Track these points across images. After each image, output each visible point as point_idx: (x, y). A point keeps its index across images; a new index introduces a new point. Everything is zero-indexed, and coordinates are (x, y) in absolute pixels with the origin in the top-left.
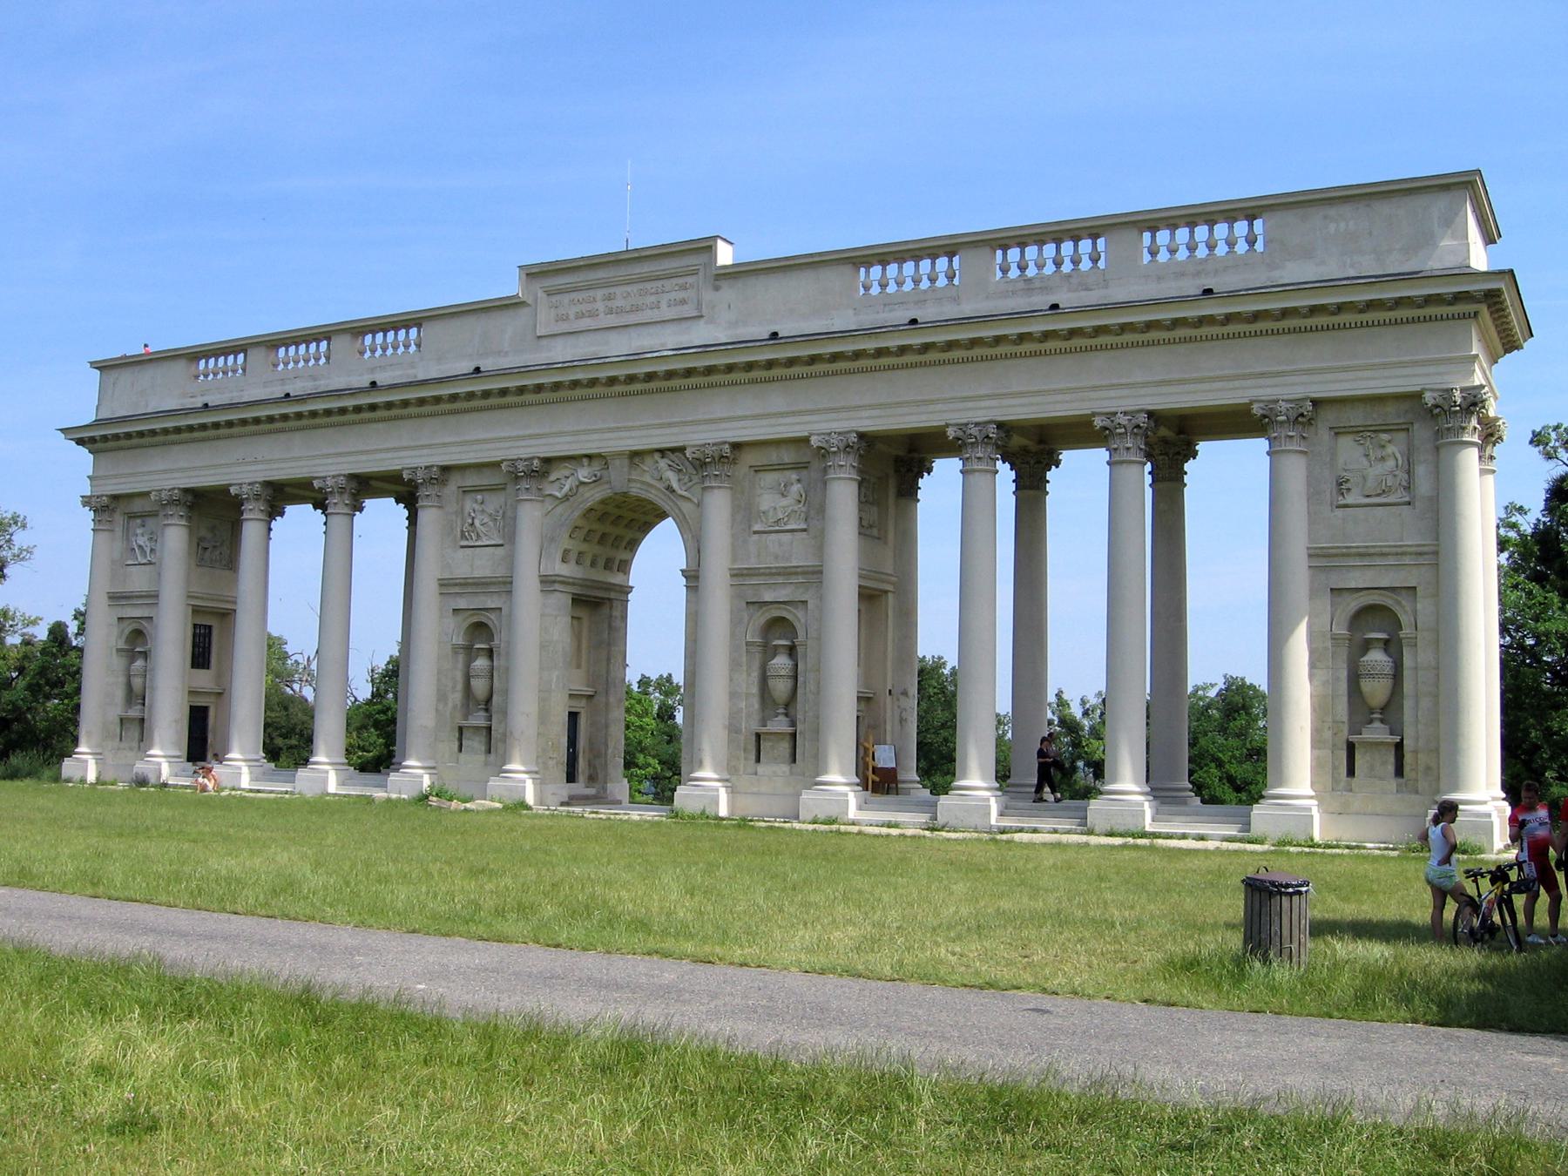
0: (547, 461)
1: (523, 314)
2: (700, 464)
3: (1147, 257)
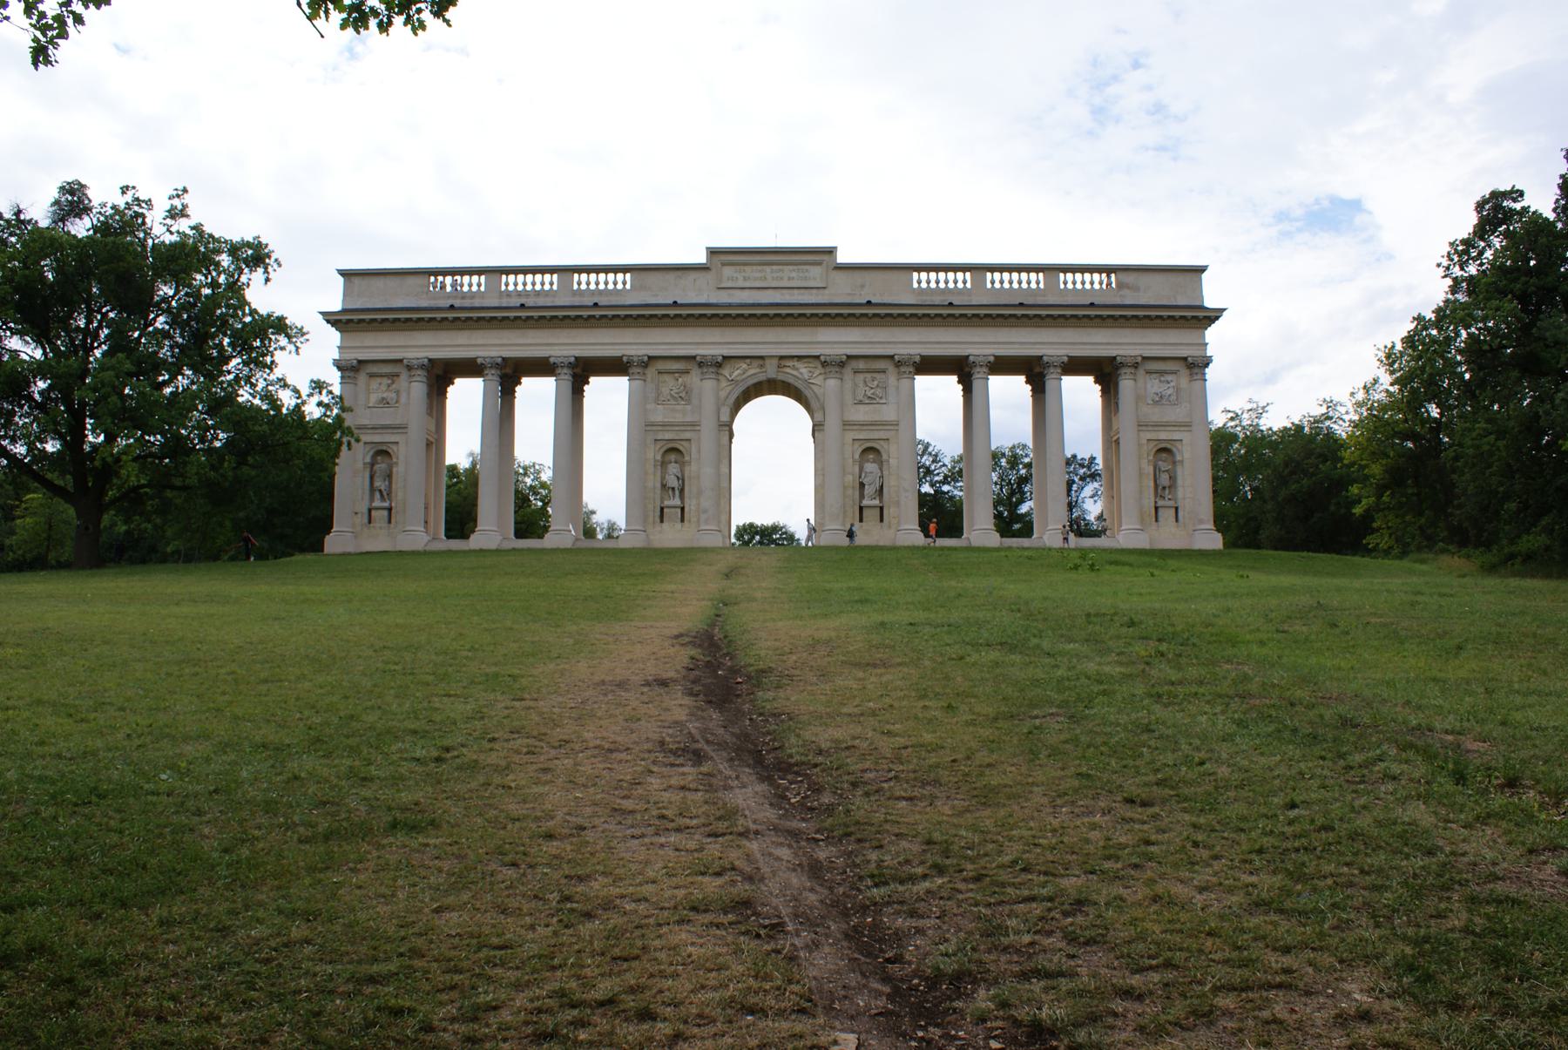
0: (725, 358)
1: (709, 276)
2: (825, 364)
3: (1062, 286)
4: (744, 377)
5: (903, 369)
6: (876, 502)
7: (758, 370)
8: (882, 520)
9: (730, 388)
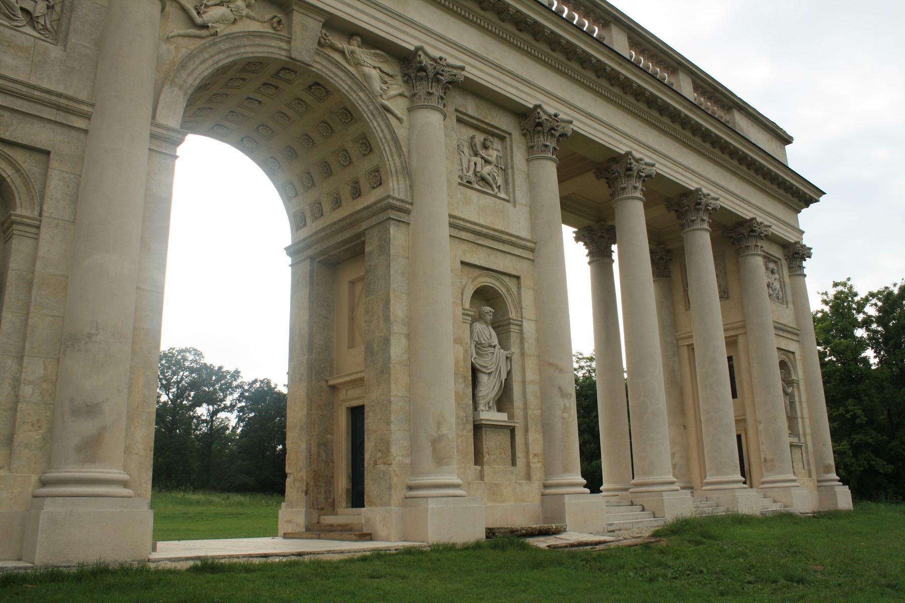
4: (235, 29)
5: (541, 140)
6: (502, 417)
7: (267, 29)
8: (514, 463)
9: (194, 44)
